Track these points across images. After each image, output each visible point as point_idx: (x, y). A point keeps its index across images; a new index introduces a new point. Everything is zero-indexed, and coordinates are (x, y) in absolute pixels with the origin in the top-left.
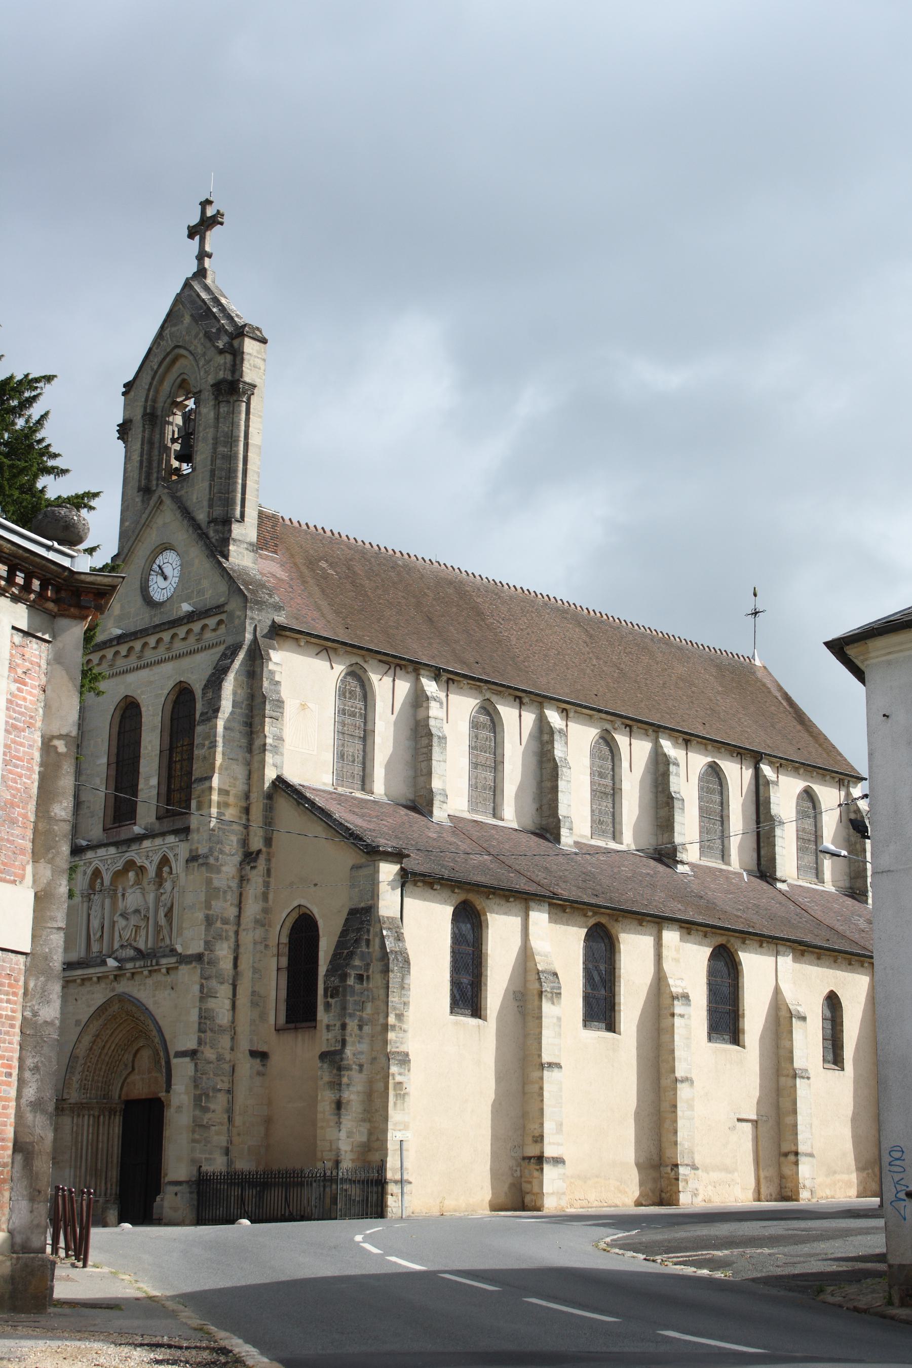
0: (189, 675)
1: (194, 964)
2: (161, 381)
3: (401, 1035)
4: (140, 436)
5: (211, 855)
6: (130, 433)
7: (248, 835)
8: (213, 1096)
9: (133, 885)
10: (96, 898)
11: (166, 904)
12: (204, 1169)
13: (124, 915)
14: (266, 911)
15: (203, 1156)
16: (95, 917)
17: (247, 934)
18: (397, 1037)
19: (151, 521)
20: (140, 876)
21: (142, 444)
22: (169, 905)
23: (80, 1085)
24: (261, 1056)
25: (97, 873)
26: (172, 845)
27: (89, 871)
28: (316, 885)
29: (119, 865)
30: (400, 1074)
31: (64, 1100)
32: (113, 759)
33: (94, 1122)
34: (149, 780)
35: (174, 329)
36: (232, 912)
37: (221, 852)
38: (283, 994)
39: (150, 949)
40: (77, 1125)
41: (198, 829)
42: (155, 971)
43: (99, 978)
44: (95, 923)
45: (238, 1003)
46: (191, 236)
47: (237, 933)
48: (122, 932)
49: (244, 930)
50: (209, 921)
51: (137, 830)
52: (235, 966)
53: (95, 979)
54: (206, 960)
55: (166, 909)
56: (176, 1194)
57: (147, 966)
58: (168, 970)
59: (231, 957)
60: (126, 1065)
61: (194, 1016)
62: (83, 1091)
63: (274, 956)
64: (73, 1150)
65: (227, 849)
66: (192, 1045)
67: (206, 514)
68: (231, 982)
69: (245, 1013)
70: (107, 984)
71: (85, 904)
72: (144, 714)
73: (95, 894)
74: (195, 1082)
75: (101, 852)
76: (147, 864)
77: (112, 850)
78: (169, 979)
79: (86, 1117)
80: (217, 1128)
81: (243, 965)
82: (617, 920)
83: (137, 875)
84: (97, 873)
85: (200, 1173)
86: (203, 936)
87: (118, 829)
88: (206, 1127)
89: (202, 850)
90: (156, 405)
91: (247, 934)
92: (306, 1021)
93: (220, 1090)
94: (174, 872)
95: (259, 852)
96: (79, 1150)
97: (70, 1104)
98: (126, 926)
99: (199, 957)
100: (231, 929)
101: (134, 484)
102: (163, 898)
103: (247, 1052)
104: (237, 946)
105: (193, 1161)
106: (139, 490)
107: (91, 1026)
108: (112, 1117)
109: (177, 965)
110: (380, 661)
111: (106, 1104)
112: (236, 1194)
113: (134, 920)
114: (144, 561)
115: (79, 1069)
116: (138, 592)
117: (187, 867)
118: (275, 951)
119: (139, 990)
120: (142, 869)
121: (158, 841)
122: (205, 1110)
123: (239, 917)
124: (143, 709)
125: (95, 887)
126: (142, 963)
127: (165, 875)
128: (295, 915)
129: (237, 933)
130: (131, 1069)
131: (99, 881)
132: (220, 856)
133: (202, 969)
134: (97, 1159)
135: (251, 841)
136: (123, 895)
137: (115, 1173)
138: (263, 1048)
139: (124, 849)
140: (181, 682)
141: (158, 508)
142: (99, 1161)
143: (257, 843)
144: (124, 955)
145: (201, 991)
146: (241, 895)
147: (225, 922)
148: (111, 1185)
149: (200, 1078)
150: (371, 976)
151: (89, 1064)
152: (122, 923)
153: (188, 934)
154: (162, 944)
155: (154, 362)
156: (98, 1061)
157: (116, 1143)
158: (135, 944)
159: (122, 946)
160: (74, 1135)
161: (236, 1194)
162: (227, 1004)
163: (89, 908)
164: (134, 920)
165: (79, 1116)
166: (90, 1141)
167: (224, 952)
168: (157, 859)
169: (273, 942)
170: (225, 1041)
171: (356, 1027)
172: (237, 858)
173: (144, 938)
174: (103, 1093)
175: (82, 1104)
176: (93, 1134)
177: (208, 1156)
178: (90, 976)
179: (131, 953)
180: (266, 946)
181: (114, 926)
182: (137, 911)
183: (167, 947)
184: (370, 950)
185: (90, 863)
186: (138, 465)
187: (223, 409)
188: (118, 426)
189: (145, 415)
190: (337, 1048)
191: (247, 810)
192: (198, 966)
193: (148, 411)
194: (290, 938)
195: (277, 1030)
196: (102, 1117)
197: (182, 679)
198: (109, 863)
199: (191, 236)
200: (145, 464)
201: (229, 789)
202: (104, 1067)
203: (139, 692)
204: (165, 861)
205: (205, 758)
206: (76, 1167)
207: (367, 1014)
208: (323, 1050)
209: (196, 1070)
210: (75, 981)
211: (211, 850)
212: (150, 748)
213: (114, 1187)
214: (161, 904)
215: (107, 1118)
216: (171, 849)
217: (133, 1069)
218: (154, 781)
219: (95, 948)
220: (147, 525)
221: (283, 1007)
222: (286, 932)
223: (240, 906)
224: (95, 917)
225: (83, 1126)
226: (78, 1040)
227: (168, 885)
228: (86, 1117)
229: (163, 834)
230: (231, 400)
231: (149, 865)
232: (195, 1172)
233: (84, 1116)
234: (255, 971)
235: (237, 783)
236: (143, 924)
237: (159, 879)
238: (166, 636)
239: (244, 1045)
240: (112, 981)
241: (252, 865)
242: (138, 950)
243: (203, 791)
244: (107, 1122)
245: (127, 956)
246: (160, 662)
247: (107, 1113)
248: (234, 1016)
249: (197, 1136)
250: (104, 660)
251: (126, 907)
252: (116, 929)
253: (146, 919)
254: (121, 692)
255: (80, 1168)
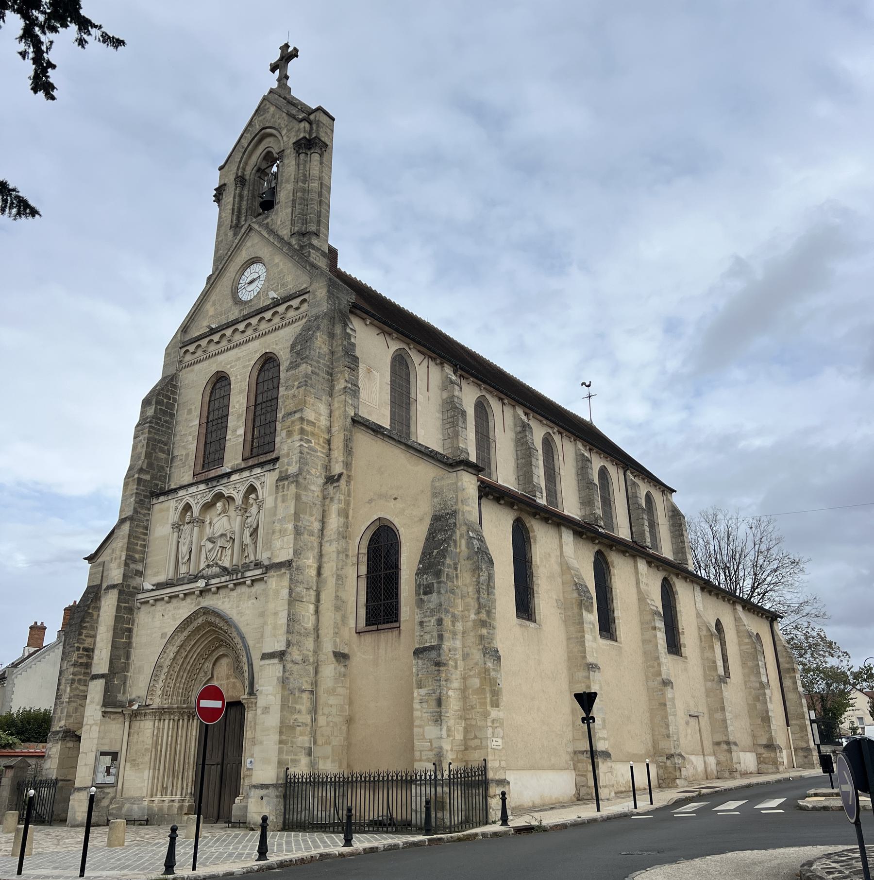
0: (274, 347)
1: (283, 571)
2: (250, 156)
3: (491, 632)
4: (233, 192)
5: (301, 474)
6: (224, 193)
7: (330, 462)
8: (298, 697)
9: (220, 514)
10: (186, 528)
11: (251, 526)
12: (291, 771)
13: (210, 540)
14: (346, 526)
15: (290, 758)
16: (184, 544)
17: (330, 545)
18: (488, 633)
19: (241, 245)
20: (227, 506)
21: (234, 198)
22: (254, 526)
23: (163, 691)
24: (341, 657)
25: (188, 507)
26: (258, 475)
27: (181, 506)
28: (395, 499)
29: (209, 497)
30: (494, 670)
31: (147, 706)
32: (204, 420)
33: (173, 725)
34: (236, 431)
35: (261, 118)
36: (317, 526)
37: (309, 473)
38: (363, 599)
39: (235, 565)
40: (158, 729)
41: (288, 455)
42: (240, 584)
43: (185, 595)
44: (184, 549)
45: (321, 608)
46: (273, 70)
47: (321, 545)
48: (208, 554)
49: (327, 541)
50: (298, 532)
51: (226, 469)
52: (319, 574)
53: (182, 596)
54: (295, 567)
55: (252, 529)
56: (262, 798)
57: (233, 580)
58: (253, 581)
59: (315, 565)
60: (206, 673)
61: (283, 620)
62: (165, 697)
63: (353, 564)
64: (153, 753)
65: (313, 471)
66: (280, 646)
67: (289, 230)
68: (315, 589)
69: (328, 616)
70: (192, 600)
71: (176, 534)
72: (232, 382)
73: (184, 525)
74: (283, 682)
75: (193, 489)
76: (234, 494)
77: (202, 487)
78: (253, 590)
79: (167, 721)
80: (301, 728)
81: (327, 572)
82: (611, 549)
83: (224, 505)
84: (188, 507)
85: (287, 776)
86: (292, 545)
87: (207, 473)
88: (292, 728)
89: (293, 469)
90: (245, 173)
91: (330, 545)
92: (387, 623)
93: (305, 690)
94: (260, 497)
95: (340, 475)
96: (159, 753)
97: (153, 709)
98: (212, 548)
99: (288, 564)
100: (314, 540)
101: (228, 222)
102: (249, 520)
103: (332, 654)
104: (321, 555)
105: (280, 763)
106: (231, 227)
107: (176, 637)
108: (191, 720)
109: (262, 576)
110: (419, 351)
111: (185, 708)
112: (320, 795)
113: (220, 542)
114: (235, 274)
115: (163, 677)
116: (230, 296)
117: (277, 486)
118: (355, 560)
119: (223, 603)
120: (231, 499)
121: (246, 474)
122: (293, 711)
123: (322, 530)
124: (232, 379)
125: (185, 519)
126: (228, 578)
127: (251, 501)
128: (374, 528)
129: (321, 545)
130: (210, 676)
131: (189, 514)
132: (308, 476)
133: (291, 575)
134: (175, 761)
135: (333, 467)
136: (210, 523)
137: (191, 774)
138: (346, 651)
139: (215, 484)
140: (266, 353)
141: (247, 234)
142: (177, 762)
143: (337, 469)
144: (210, 573)
145: (290, 594)
146: (324, 511)
147: (311, 534)
148: (187, 785)
149: (287, 678)
150: (459, 575)
151: (172, 672)
152: (210, 545)
153: (277, 543)
154: (247, 561)
155: (245, 142)
156: (180, 669)
157: (193, 745)
158: (220, 563)
159: (208, 566)
160: (155, 738)
161: (320, 795)
162: (312, 608)
163: (179, 537)
164: (220, 542)
165: (160, 720)
166: (169, 743)
167: (309, 562)
168: (243, 488)
169: (353, 550)
170: (309, 644)
171: (450, 623)
172: (321, 481)
173: (229, 557)
174: (183, 698)
175: (163, 709)
176: (172, 736)
177: (293, 757)
178: (177, 593)
179: (216, 570)
180: (347, 556)
181: (200, 551)
182: (222, 535)
183: (251, 562)
184: (458, 550)
185: (182, 500)
186: (231, 212)
187: (302, 156)
188: (215, 190)
189: (237, 177)
190: (433, 644)
191: (329, 442)
192: (287, 572)
193: (239, 175)
194: (368, 548)
195: (358, 633)
196: (181, 720)
197: (268, 351)
198: (198, 498)
199: (273, 70)
200: (235, 211)
201: (315, 421)
202: (185, 675)
203: (229, 367)
204: (252, 489)
205: (294, 396)
206: (154, 769)
207: (458, 611)
208: (417, 646)
209: (284, 671)
210: (163, 599)
211: (300, 469)
212: (237, 407)
213: (189, 788)
214: (246, 526)
215: (186, 721)
216: (258, 478)
217: (212, 676)
218: (241, 431)
219: (183, 569)
220: (238, 248)
221: (362, 612)
222: (365, 543)
223: (323, 522)
224: (184, 544)
225: (163, 729)
226: (164, 651)
227: (254, 510)
228: (167, 721)
229: (251, 468)
230: (309, 153)
231: (236, 494)
232: (282, 775)
233: (164, 720)
234: (339, 577)
235: (322, 418)
236: (228, 545)
237: (244, 509)
238: (254, 321)
239: (328, 647)
240: (198, 596)
241: (335, 485)
242: (225, 569)
243: (293, 422)
244: (185, 726)
245: (213, 574)
246: (247, 342)
247: (186, 717)
248: (318, 620)
249: (284, 738)
250: (200, 349)
251: (213, 533)
252: (203, 552)
253: (232, 541)
254: (214, 369)
255: (159, 769)
